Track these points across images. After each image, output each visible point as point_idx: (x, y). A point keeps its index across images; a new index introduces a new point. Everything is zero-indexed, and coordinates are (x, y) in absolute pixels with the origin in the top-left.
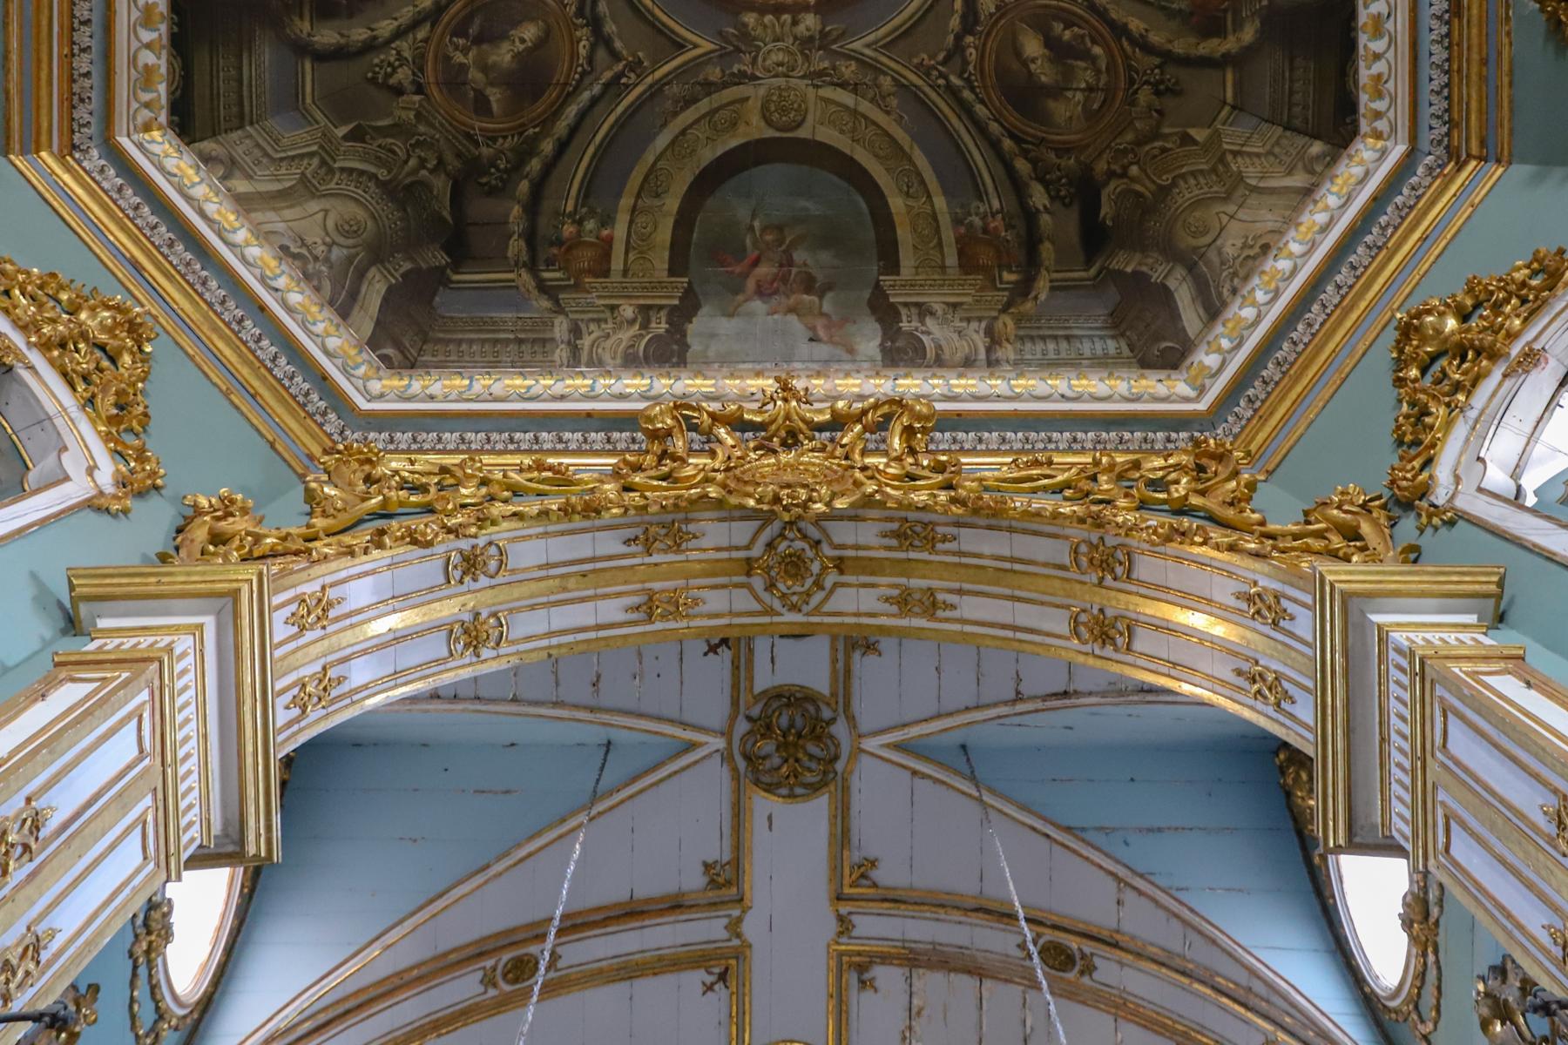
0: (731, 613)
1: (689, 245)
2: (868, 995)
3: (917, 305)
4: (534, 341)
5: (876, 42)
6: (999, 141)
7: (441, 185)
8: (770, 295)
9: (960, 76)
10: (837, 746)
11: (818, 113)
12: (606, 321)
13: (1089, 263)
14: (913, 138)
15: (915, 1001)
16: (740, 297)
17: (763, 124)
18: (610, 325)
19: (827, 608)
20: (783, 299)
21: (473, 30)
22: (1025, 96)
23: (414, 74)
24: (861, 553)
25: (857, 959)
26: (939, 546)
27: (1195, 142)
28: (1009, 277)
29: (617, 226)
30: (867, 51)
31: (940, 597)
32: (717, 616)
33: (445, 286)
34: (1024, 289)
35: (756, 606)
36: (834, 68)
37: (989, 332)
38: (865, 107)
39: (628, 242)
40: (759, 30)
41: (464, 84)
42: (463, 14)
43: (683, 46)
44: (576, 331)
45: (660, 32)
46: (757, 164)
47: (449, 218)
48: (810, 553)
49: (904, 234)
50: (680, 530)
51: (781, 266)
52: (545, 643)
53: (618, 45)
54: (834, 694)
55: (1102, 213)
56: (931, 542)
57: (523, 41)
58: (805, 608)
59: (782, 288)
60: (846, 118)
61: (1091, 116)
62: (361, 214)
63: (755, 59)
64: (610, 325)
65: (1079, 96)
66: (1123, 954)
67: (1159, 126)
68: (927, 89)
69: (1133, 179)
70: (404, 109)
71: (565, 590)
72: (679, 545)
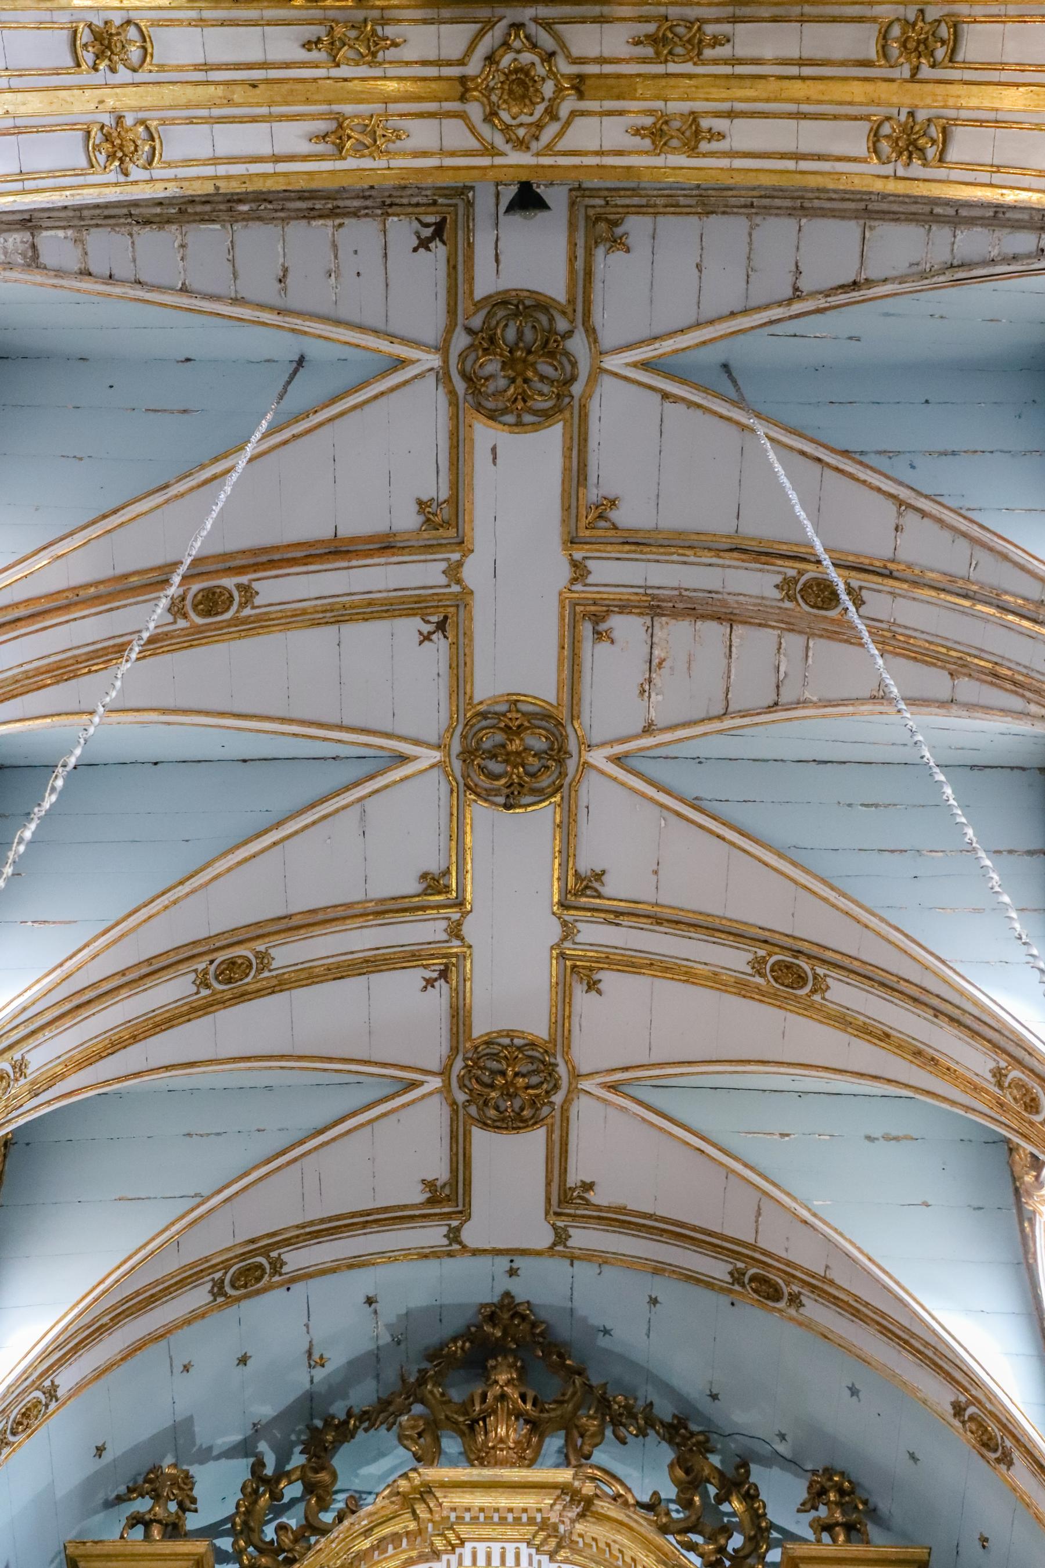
0: (442, 152)
2: (604, 647)
10: (574, 364)
15: (656, 652)
19: (561, 146)
24: (608, 69)
25: (593, 608)
26: (708, 53)
31: (705, 123)
32: (425, 154)
35: (473, 144)
48: (541, 70)
50: (374, 32)
52: (209, 171)
54: (572, 301)
56: (696, 47)
58: (535, 146)
66: (897, 584)
71: (230, 102)
72: (374, 54)
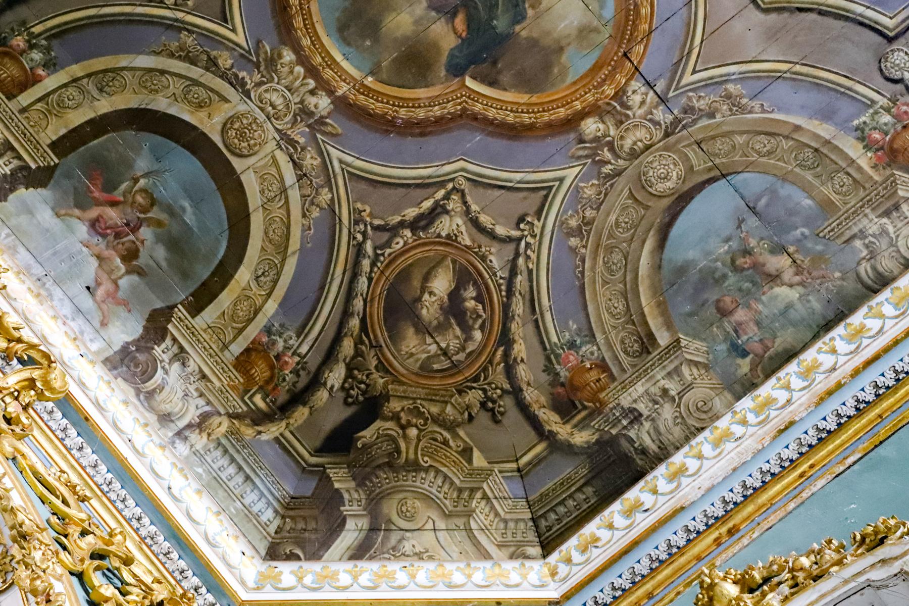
1: (84, 143)
3: (182, 348)
5: (348, 165)
6: (352, 314)
9: (375, 248)
13: (319, 451)
14: (302, 249)
16: (77, 212)
17: (219, 127)
20: (103, 246)
22: (399, 308)
27: (470, 461)
28: (258, 399)
29: (53, 77)
30: (336, 164)
34: (259, 419)
36: (303, 149)
38: (295, 195)
43: (226, 22)
49: (225, 299)
51: (127, 225)
55: (360, 434)
59: (111, 238)
60: (275, 187)
61: (425, 369)
63: (261, 83)
67: (458, 425)
68: (345, 232)
69: (405, 436)
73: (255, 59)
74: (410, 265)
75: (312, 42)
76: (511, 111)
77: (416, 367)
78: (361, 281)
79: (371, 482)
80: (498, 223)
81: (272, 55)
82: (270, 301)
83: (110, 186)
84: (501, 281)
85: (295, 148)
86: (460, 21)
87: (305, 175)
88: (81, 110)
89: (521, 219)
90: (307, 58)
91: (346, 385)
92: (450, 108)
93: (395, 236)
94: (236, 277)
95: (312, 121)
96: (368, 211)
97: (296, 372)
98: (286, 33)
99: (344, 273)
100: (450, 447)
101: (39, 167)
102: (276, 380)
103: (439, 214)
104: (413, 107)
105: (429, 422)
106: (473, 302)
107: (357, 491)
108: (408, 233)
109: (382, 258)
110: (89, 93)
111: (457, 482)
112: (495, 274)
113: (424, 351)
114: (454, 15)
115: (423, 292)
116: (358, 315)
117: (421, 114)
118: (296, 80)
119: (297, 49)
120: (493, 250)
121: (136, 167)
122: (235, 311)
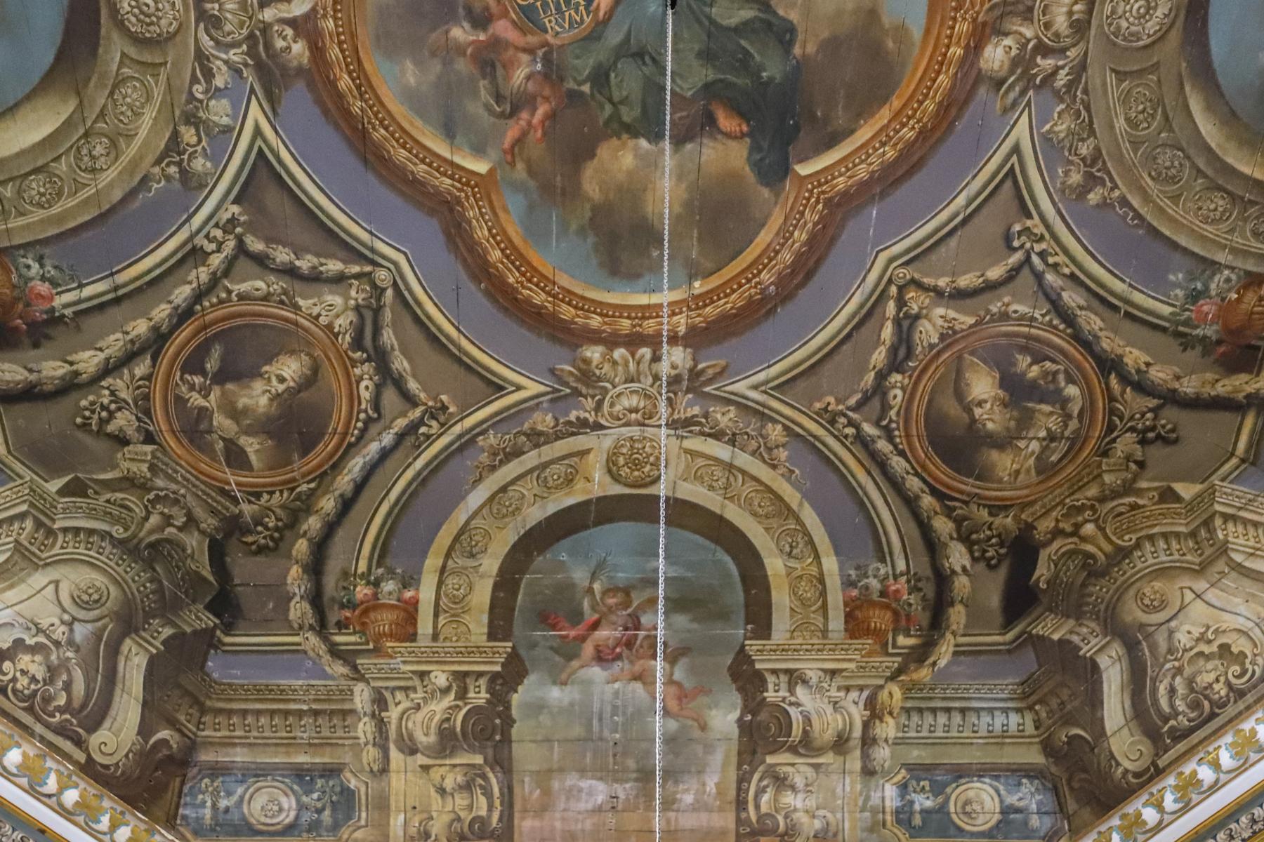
3: (787, 671)
4: (333, 712)
6: (917, 497)
7: (193, 542)
8: (614, 660)
9: (877, 424)
11: (682, 466)
12: (414, 689)
13: (1008, 624)
14: (805, 495)
16: (575, 664)
17: (608, 479)
18: (420, 694)
21: (212, 365)
22: (959, 446)
23: (139, 419)
27: (1177, 498)
28: (902, 640)
33: (216, 648)
34: (920, 655)
36: (706, 415)
37: (871, 703)
38: (744, 460)
39: (437, 605)
40: (607, 367)
41: (210, 432)
42: (194, 343)
44: (380, 702)
45: (468, 368)
46: (596, 524)
47: (211, 578)
49: (781, 598)
51: (626, 629)
53: (413, 385)
55: (1034, 578)
57: (282, 380)
59: (626, 652)
60: (718, 472)
61: (1045, 469)
62: (100, 580)
63: (599, 406)
64: (420, 694)
65: (1035, 446)
67: (1134, 480)
68: (831, 441)
69: (1084, 539)
70: (136, 459)
73: (568, 391)
74: (930, 401)
75: (601, 315)
76: (883, 144)
77: (1034, 477)
78: (894, 464)
79: (1088, 604)
80: (986, 269)
81: (579, 370)
82: (824, 560)
83: (576, 616)
84: (1047, 318)
85: (700, 424)
86: (726, 122)
87: (734, 434)
88: (477, 588)
89: (1008, 239)
90: (615, 334)
91: (976, 554)
92: (811, 217)
93: (885, 394)
94: (769, 573)
95: (685, 383)
96: (832, 400)
97: (914, 589)
98: (569, 336)
99: (869, 473)
100: (1144, 506)
101: (503, 665)
102: (902, 612)
103: (911, 327)
104: (771, 260)
105: (1097, 505)
106: (1035, 368)
107: (1080, 625)
108: (896, 378)
109: (894, 425)
110: (466, 568)
111: (1183, 529)
112: (1033, 319)
113: (1026, 458)
114: (711, 120)
115: (969, 411)
116: (923, 492)
117: (787, 257)
118: (626, 364)
119: (594, 337)
120: (1006, 300)
121: (577, 581)
122: (800, 599)
